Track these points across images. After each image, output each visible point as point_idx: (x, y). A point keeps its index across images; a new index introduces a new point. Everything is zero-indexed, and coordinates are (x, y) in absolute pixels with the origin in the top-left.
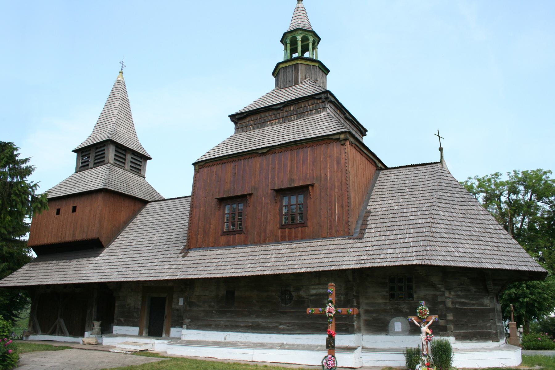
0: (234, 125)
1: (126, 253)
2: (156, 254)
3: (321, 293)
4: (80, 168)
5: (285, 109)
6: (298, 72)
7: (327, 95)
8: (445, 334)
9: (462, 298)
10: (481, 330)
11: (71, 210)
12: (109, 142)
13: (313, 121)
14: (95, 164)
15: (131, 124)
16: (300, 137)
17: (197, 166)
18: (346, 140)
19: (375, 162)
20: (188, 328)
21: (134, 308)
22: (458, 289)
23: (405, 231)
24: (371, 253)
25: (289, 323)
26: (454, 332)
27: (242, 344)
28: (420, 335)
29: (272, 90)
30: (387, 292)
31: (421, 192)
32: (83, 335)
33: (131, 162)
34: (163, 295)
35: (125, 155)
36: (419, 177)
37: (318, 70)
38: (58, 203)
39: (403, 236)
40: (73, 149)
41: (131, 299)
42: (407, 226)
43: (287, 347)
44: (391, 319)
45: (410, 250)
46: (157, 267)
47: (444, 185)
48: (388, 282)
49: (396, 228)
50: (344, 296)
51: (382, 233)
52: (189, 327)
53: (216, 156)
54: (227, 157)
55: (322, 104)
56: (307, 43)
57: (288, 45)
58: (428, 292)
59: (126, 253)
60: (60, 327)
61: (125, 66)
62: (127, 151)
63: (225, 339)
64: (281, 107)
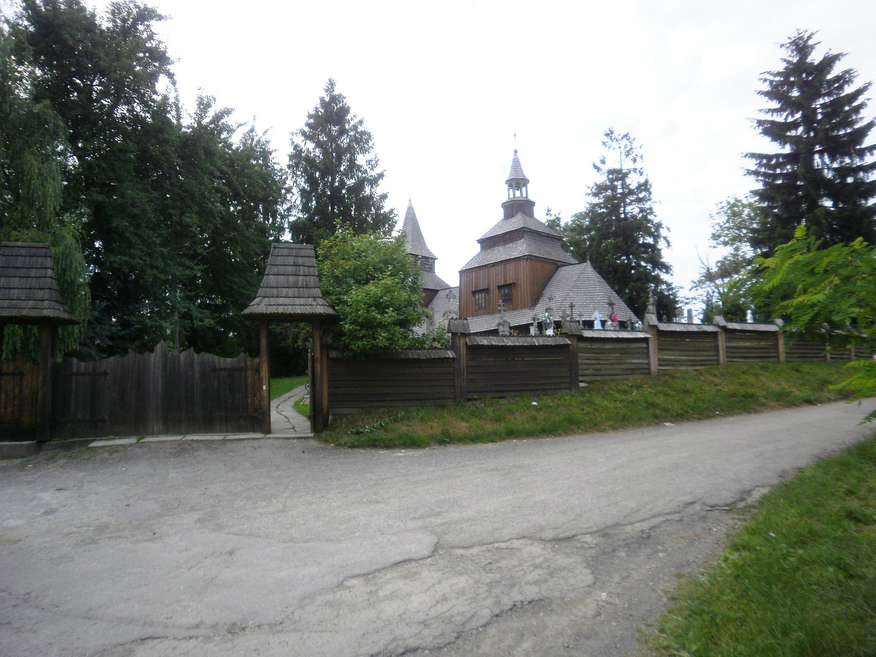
16: (508, 257)
18: (527, 259)
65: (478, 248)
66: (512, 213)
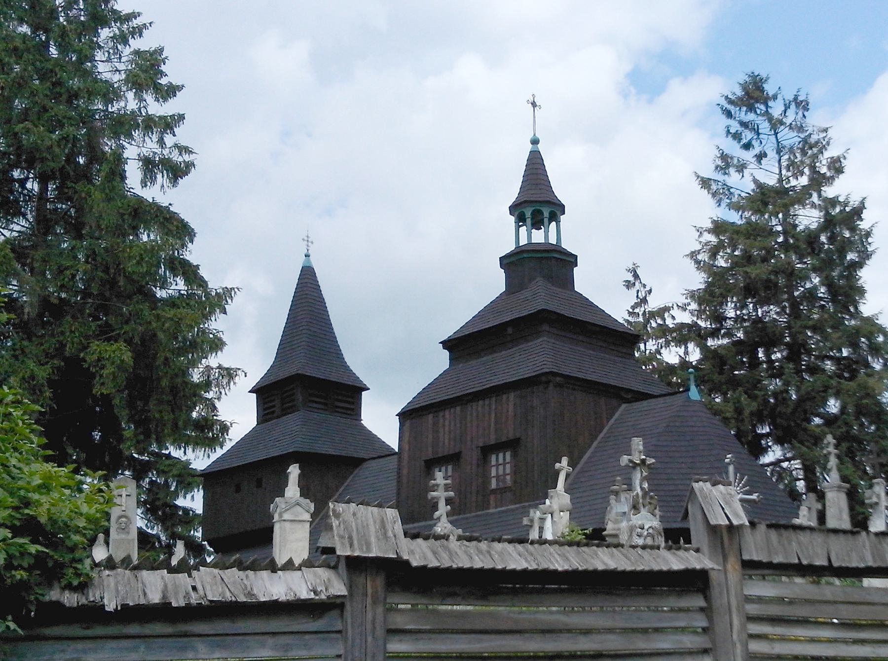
14: (283, 410)
18: (548, 382)
65: (445, 356)
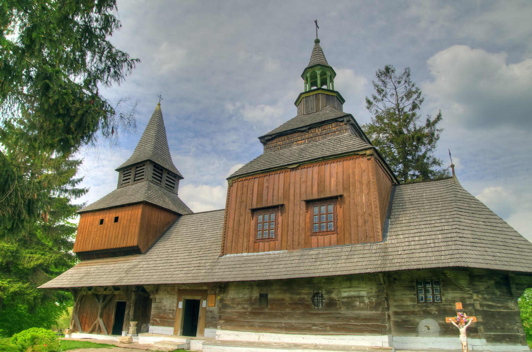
0: (263, 146)
1: (163, 259)
2: (192, 259)
3: (352, 296)
4: (122, 184)
5: (310, 131)
6: (319, 101)
7: (349, 118)
8: (476, 335)
9: (488, 300)
10: (508, 332)
11: (113, 220)
12: (148, 162)
13: (337, 140)
15: (166, 148)
17: (231, 181)
19: (391, 178)
20: (222, 329)
21: (170, 310)
22: (485, 292)
23: (434, 237)
24: (405, 256)
25: (322, 324)
26: (484, 333)
27: (277, 345)
28: (459, 337)
29: (296, 116)
30: (415, 295)
31: (440, 203)
32: (120, 334)
33: (167, 180)
34: (197, 298)
35: (161, 174)
36: (435, 191)
37: (336, 99)
38: (102, 213)
39: (432, 241)
40: (116, 168)
41: (167, 301)
42: (434, 232)
43: (321, 347)
44: (420, 321)
45: (443, 253)
46: (193, 272)
47: (460, 196)
48: (415, 285)
49: (423, 234)
50: (376, 298)
51: (410, 239)
52: (224, 328)
53: (249, 172)
54: (259, 172)
55: (345, 126)
56: (325, 77)
57: (309, 79)
58: (456, 295)
59: (163, 259)
60: (99, 326)
61: (162, 99)
62: (164, 170)
63: (259, 339)
64: (307, 130)
66: (317, 105)
